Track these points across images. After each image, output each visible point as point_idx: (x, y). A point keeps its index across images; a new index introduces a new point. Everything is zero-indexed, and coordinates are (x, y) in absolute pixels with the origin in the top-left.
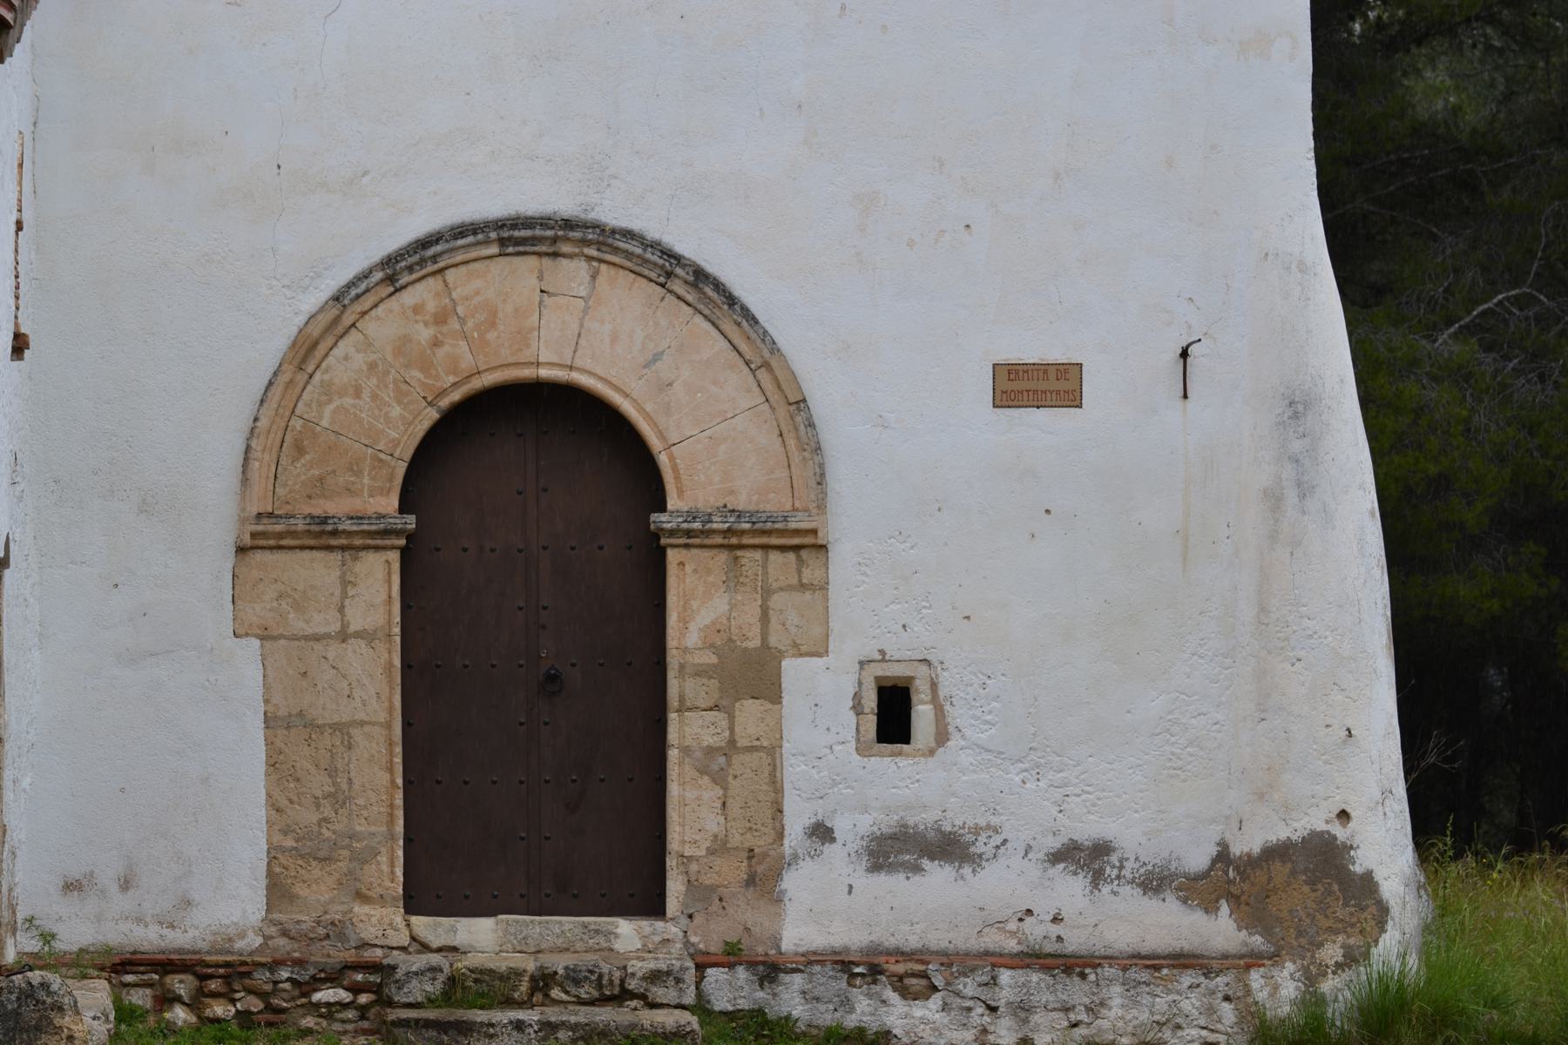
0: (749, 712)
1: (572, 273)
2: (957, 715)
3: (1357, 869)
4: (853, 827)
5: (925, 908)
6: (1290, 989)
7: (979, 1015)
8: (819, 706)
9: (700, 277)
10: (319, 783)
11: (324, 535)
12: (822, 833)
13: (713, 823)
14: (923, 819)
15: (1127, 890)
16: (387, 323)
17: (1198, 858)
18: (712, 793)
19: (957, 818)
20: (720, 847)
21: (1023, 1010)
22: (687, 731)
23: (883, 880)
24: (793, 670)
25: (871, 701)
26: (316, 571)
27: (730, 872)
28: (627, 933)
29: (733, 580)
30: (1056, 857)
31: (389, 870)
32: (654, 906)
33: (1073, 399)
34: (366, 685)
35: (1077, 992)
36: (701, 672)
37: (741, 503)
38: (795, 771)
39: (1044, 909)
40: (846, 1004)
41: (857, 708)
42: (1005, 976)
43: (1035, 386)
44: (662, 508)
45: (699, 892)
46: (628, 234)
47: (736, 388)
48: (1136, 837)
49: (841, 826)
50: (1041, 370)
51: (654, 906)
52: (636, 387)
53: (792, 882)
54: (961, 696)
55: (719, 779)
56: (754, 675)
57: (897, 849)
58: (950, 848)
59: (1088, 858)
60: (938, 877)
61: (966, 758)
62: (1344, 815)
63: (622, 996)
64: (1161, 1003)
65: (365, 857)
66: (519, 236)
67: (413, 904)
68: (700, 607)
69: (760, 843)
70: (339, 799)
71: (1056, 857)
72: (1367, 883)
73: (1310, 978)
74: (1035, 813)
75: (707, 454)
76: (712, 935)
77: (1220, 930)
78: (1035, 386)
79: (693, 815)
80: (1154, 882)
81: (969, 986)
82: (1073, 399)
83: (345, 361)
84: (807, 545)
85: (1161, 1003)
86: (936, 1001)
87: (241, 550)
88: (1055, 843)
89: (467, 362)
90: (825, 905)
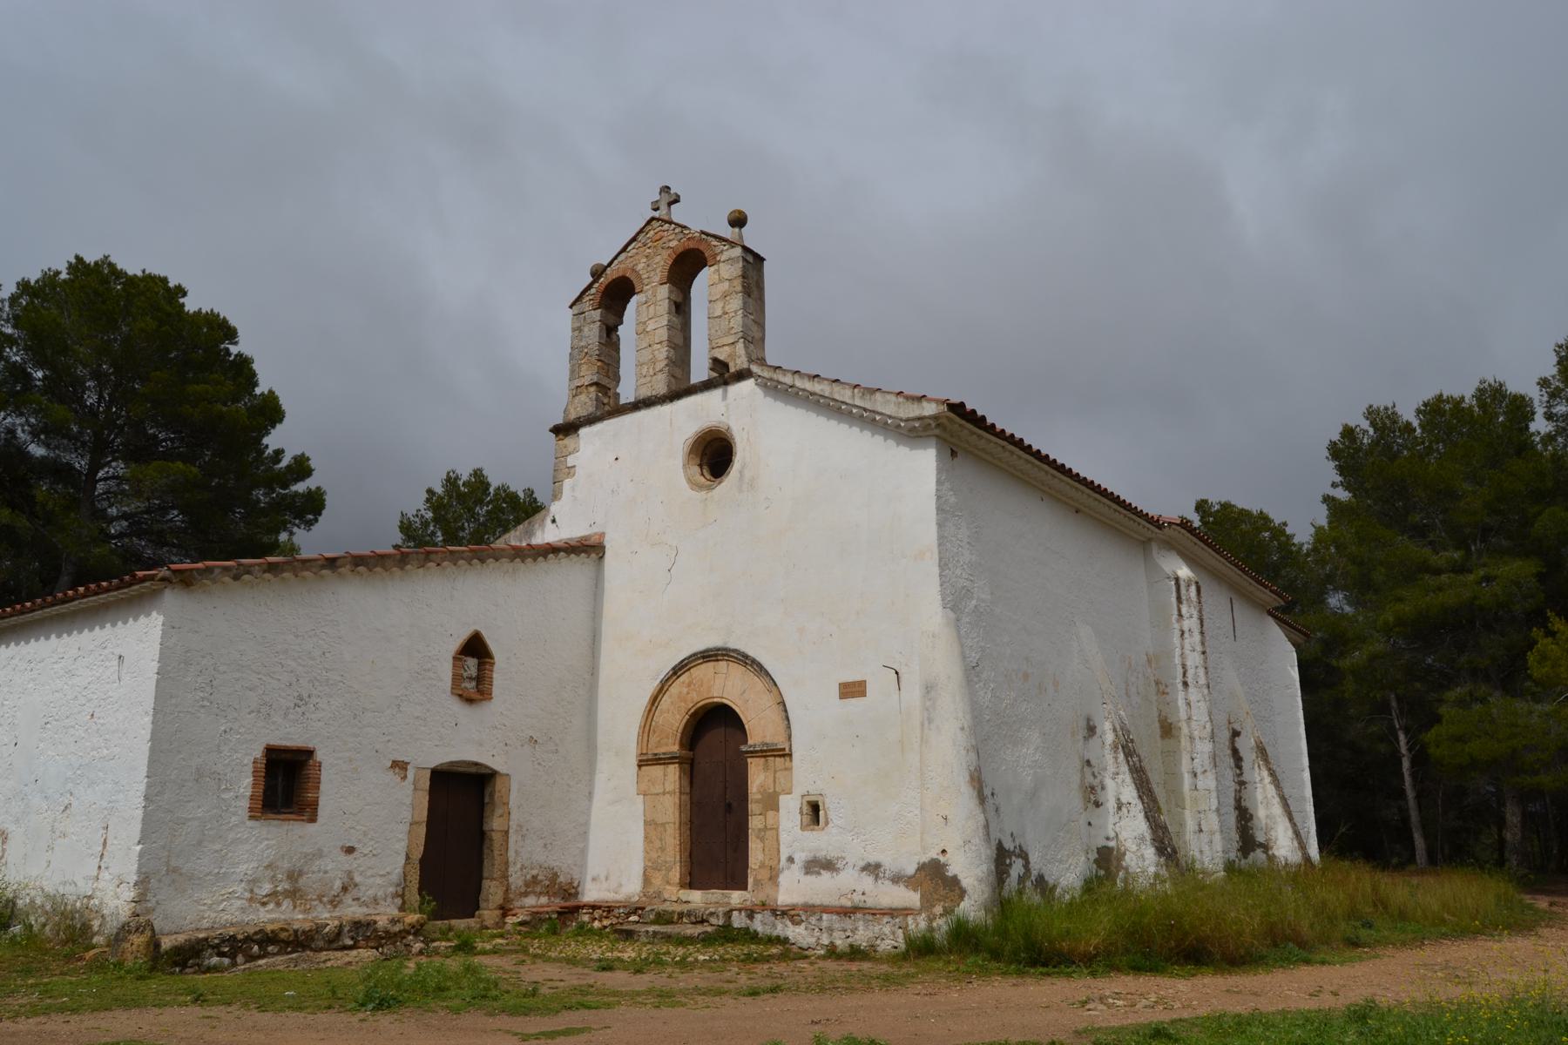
0: (771, 814)
1: (722, 665)
2: (831, 815)
3: (950, 874)
4: (800, 857)
5: (822, 889)
6: (923, 925)
7: (817, 932)
8: (790, 810)
9: (754, 661)
10: (658, 844)
11: (657, 760)
12: (791, 860)
13: (761, 857)
14: (821, 854)
15: (887, 882)
16: (676, 688)
17: (911, 869)
18: (760, 846)
19: (832, 854)
20: (762, 866)
21: (830, 930)
22: (755, 823)
23: (811, 878)
24: (783, 799)
25: (806, 809)
26: (657, 771)
27: (764, 874)
28: (736, 897)
29: (766, 768)
30: (864, 869)
31: (676, 875)
32: (745, 888)
33: (863, 694)
34: (670, 809)
35: (848, 923)
36: (757, 801)
37: (768, 740)
38: (783, 837)
39: (859, 889)
40: (774, 926)
41: (801, 813)
42: (825, 916)
43: (853, 690)
44: (746, 742)
45: (757, 882)
46: (735, 651)
47: (767, 701)
48: (889, 862)
49: (797, 857)
50: (854, 684)
51: (745, 888)
52: (740, 703)
53: (782, 879)
54: (830, 808)
55: (762, 840)
56: (771, 803)
57: (819, 865)
58: (829, 865)
59: (873, 869)
60: (826, 875)
61: (834, 831)
62: (944, 851)
63: (670, 922)
64: (877, 929)
65: (669, 870)
66: (709, 656)
67: (682, 886)
68: (758, 777)
69: (773, 863)
70: (662, 849)
71: (864, 869)
72: (955, 881)
73: (931, 920)
74: (856, 851)
75: (760, 726)
76: (761, 897)
77: (912, 898)
78: (853, 690)
79: (756, 854)
80: (896, 879)
81: (813, 920)
82: (863, 694)
83: (666, 701)
84: (786, 754)
85: (877, 929)
86: (803, 926)
87: (640, 766)
88: (862, 864)
89: (696, 699)
90: (792, 888)
